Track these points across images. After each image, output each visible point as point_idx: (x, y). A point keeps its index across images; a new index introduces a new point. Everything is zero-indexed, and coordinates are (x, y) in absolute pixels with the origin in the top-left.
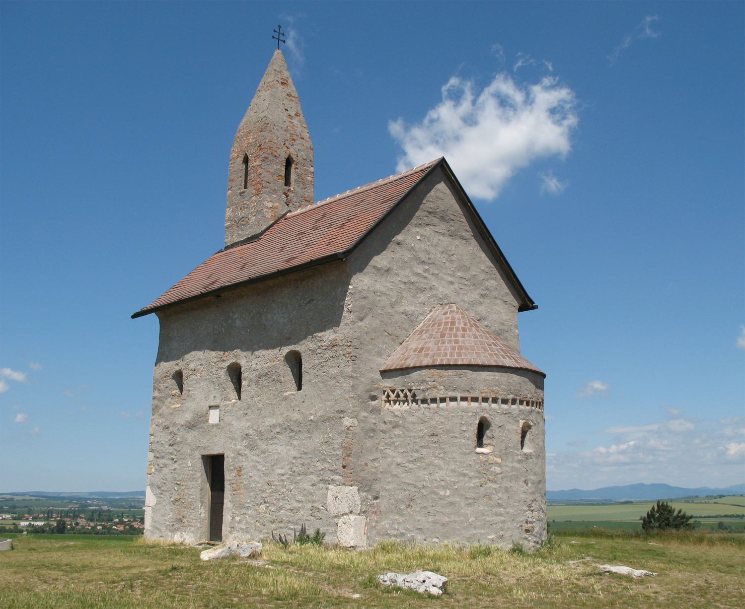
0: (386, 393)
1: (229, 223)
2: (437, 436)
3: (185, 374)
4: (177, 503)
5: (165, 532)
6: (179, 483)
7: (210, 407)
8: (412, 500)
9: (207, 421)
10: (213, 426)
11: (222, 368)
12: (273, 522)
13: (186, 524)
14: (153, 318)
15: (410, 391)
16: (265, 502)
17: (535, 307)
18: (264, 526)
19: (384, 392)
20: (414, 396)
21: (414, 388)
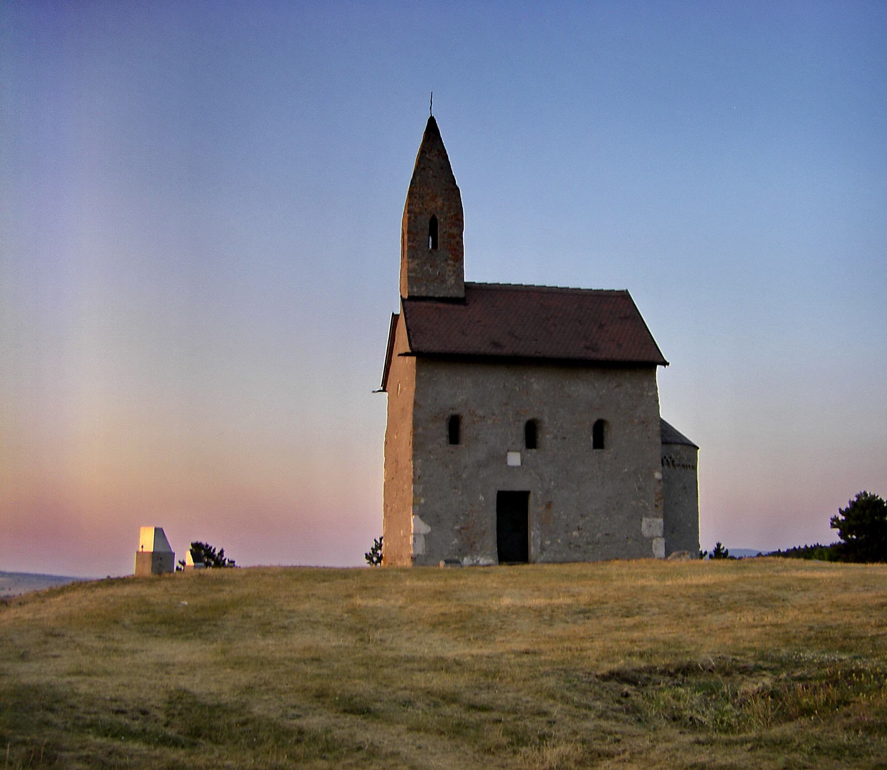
4: (463, 531)
7: (508, 451)
9: (506, 463)
10: (513, 467)
12: (588, 543)
15: (670, 458)
20: (673, 462)
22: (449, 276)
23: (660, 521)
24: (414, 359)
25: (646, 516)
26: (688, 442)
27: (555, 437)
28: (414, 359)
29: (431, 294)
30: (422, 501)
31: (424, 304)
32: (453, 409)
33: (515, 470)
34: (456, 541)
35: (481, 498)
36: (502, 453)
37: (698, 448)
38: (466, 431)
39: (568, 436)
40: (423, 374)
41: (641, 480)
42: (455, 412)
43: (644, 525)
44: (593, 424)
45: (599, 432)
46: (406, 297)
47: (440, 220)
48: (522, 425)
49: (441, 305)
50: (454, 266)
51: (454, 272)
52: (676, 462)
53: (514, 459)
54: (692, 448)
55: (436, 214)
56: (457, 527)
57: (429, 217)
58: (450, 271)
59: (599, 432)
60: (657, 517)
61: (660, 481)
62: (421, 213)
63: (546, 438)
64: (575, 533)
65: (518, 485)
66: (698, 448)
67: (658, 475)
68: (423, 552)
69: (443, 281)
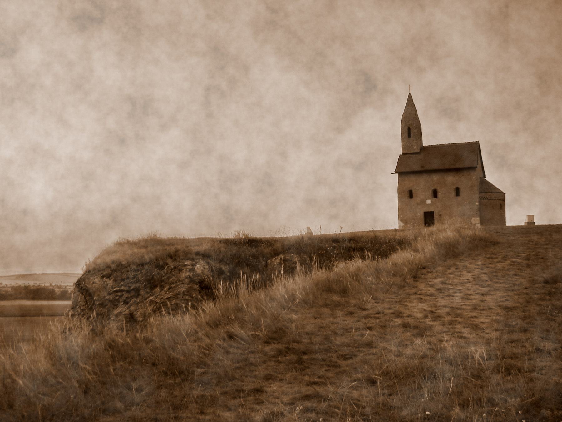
3: (414, 191)
23: (478, 218)
24: (397, 174)
25: (473, 217)
26: (499, 191)
28: (397, 174)
29: (409, 152)
30: (401, 216)
37: (505, 194)
42: (410, 189)
43: (472, 220)
45: (457, 192)
46: (401, 154)
47: (411, 128)
53: (429, 202)
54: (502, 194)
56: (412, 223)
57: (407, 128)
59: (457, 192)
60: (477, 217)
61: (477, 205)
63: (439, 195)
65: (431, 209)
66: (505, 194)
67: (477, 204)
69: (413, 148)
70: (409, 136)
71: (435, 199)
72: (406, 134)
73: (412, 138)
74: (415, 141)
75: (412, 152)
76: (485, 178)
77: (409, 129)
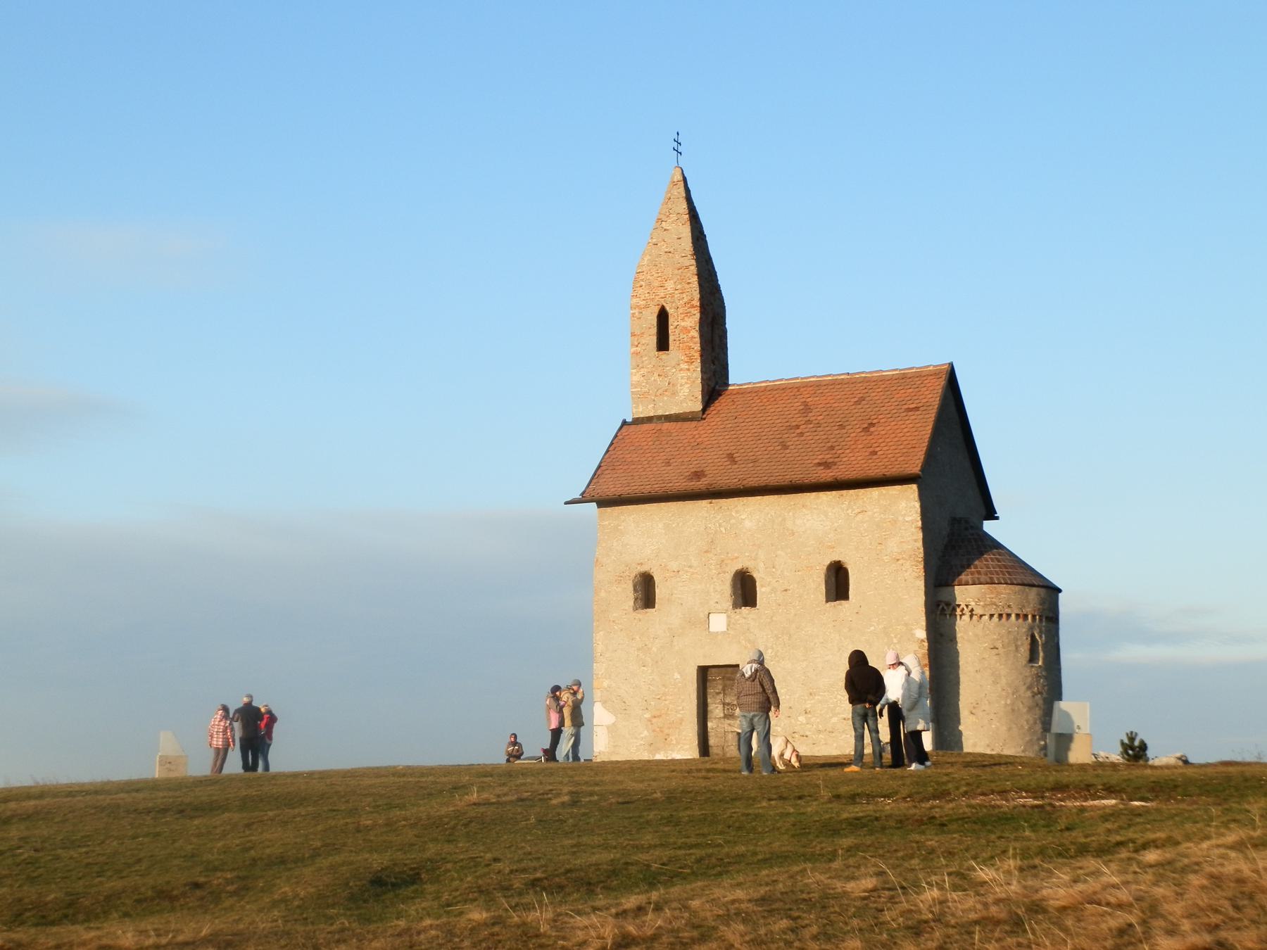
0: (941, 607)
1: (639, 389)
2: (997, 649)
4: (654, 720)
5: (635, 753)
6: (658, 697)
8: (974, 708)
11: (724, 572)
12: (819, 732)
13: (674, 742)
14: (594, 504)
15: (967, 606)
16: (806, 713)
17: (997, 518)
18: (807, 736)
19: (938, 605)
20: (972, 610)
21: (973, 603)
22: (681, 385)
27: (774, 590)
29: (660, 413)
31: (646, 426)
32: (642, 564)
33: (720, 637)
34: (646, 733)
35: (677, 676)
36: (702, 615)
37: (1060, 591)
38: (660, 592)
39: (791, 587)
40: (607, 523)
41: (895, 641)
44: (825, 568)
48: (728, 578)
49: (667, 425)
50: (688, 370)
51: (689, 378)
52: (978, 611)
53: (718, 623)
55: (665, 304)
56: (647, 715)
57: (656, 310)
58: (682, 378)
62: (647, 307)
64: (802, 719)
68: (606, 747)
69: (674, 394)
70: (663, 344)
71: (745, 610)
72: (653, 340)
73: (675, 351)
74: (684, 366)
75: (674, 410)
76: (989, 527)
77: (663, 317)
